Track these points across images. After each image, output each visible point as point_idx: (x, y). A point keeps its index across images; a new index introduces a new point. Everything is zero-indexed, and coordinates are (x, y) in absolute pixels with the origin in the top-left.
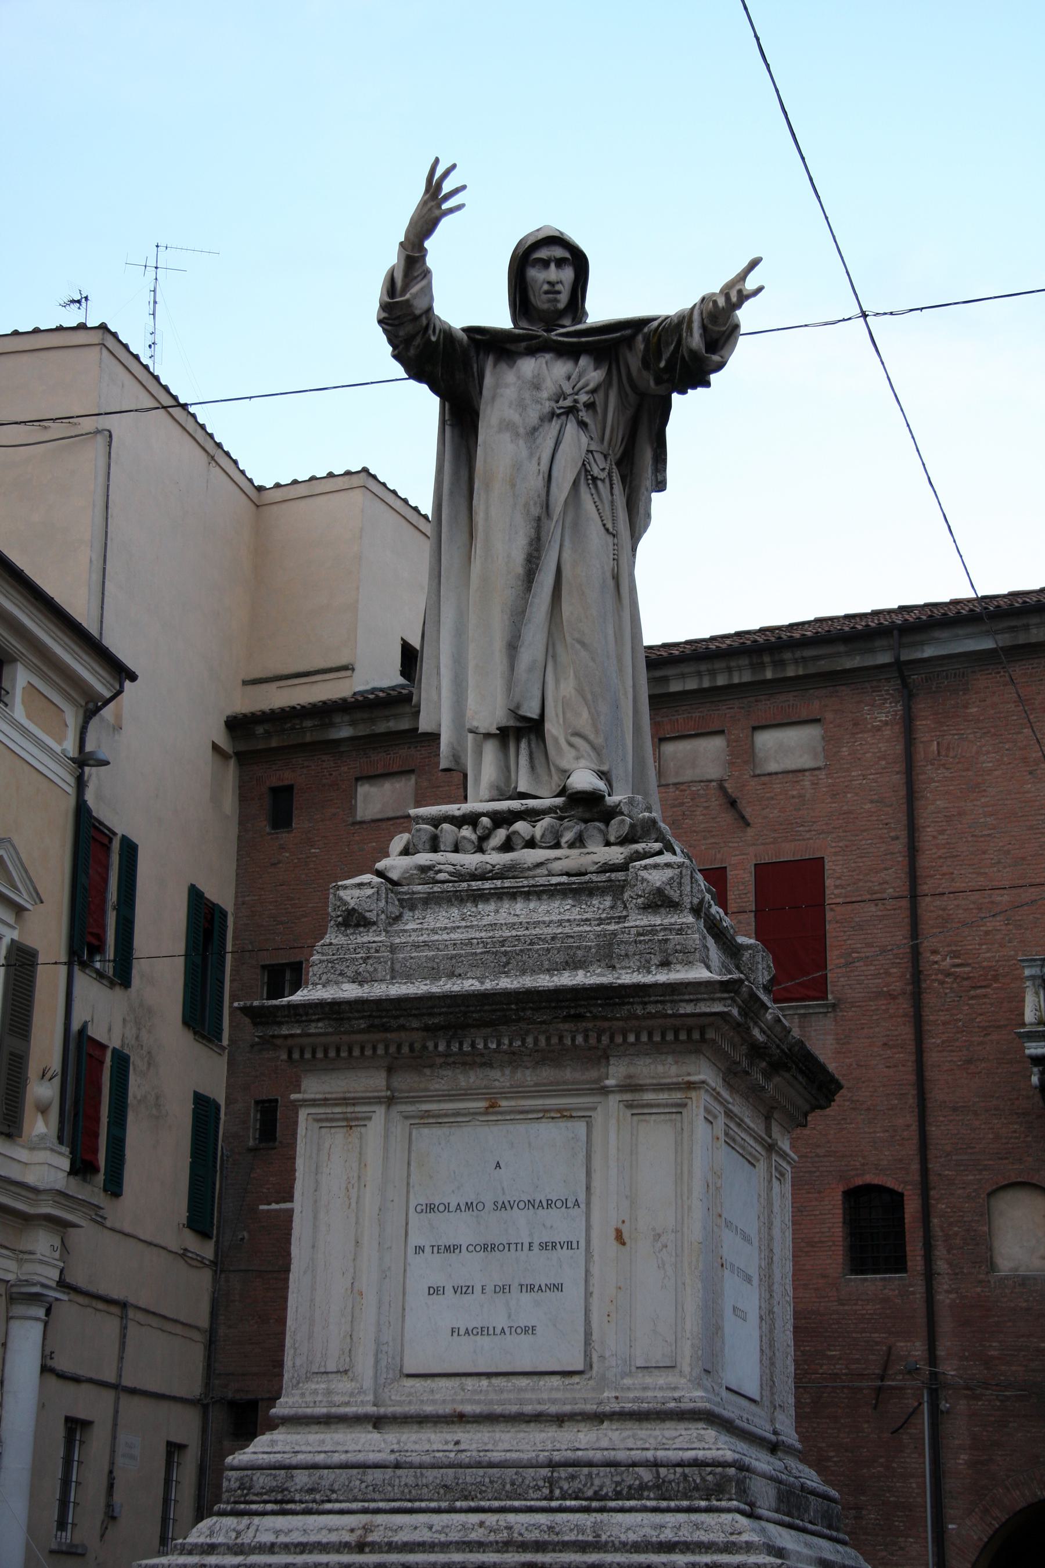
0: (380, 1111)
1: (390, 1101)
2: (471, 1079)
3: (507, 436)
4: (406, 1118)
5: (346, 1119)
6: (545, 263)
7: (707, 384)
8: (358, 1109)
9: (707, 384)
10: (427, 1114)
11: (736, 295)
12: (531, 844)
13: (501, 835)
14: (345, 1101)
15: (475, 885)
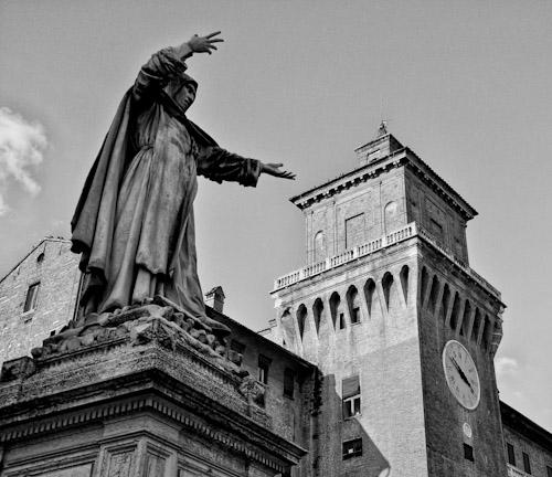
0: (174, 452)
1: (179, 450)
2: (204, 452)
3: (176, 148)
4: (179, 462)
5: (159, 452)
6: (191, 91)
7: (220, 182)
8: (167, 448)
9: (220, 182)
10: (187, 464)
11: (271, 171)
12: (207, 343)
13: (196, 333)
14: (164, 442)
15: (196, 352)
